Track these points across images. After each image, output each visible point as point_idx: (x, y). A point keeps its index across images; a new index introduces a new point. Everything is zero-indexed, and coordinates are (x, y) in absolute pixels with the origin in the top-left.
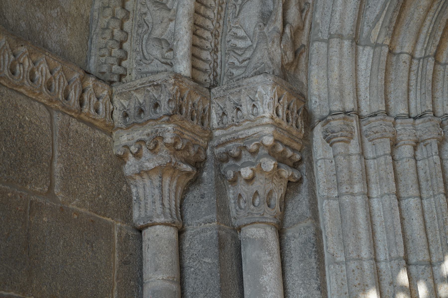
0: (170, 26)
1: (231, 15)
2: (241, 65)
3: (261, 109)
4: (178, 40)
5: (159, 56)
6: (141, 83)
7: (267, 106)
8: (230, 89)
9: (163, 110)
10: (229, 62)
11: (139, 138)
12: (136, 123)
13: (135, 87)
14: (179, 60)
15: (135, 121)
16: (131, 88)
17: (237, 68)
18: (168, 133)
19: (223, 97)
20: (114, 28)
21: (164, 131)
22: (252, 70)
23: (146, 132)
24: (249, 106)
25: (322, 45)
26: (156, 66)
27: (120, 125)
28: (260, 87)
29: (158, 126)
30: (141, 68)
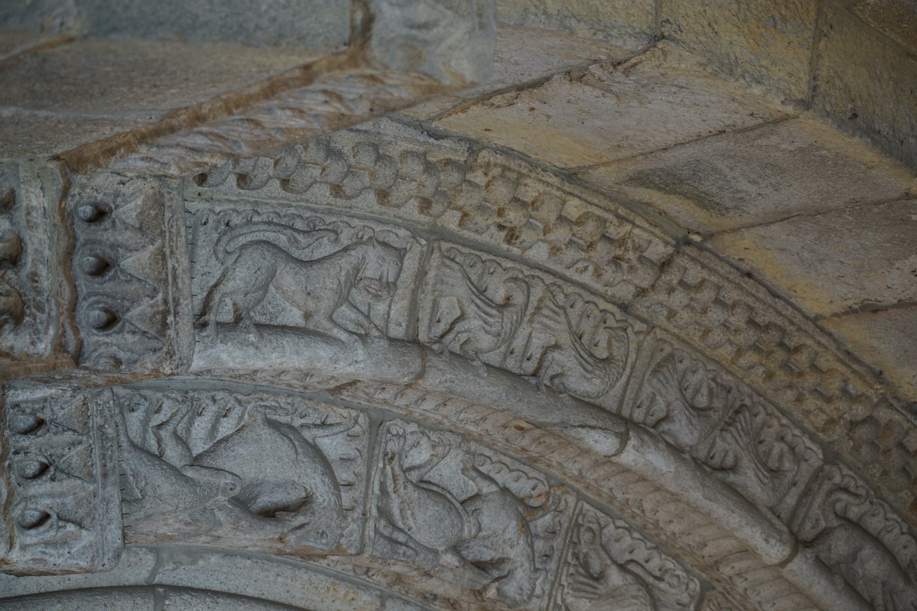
0: (295, 309)
1: (273, 404)
2: (150, 429)
3: (35, 540)
4: (257, 348)
5: (228, 286)
6: (179, 271)
7: (39, 556)
8: (103, 447)
9: (96, 338)
10: (165, 400)
11: (30, 249)
12: (74, 246)
13: (172, 252)
14: (209, 352)
15: (78, 244)
16: (171, 239)
17: (145, 422)
18: (28, 341)
19: (86, 424)
20: (324, 170)
21: (37, 332)
22: (133, 467)
23: (43, 271)
24: (48, 501)
25: (144, 572)
26: (206, 269)
27: (76, 192)
28: (92, 538)
29: (53, 313)
30: (209, 225)
